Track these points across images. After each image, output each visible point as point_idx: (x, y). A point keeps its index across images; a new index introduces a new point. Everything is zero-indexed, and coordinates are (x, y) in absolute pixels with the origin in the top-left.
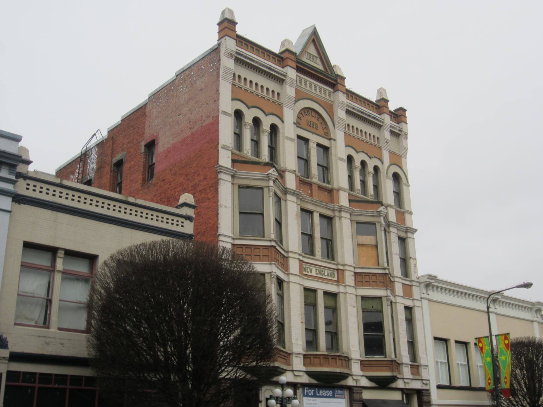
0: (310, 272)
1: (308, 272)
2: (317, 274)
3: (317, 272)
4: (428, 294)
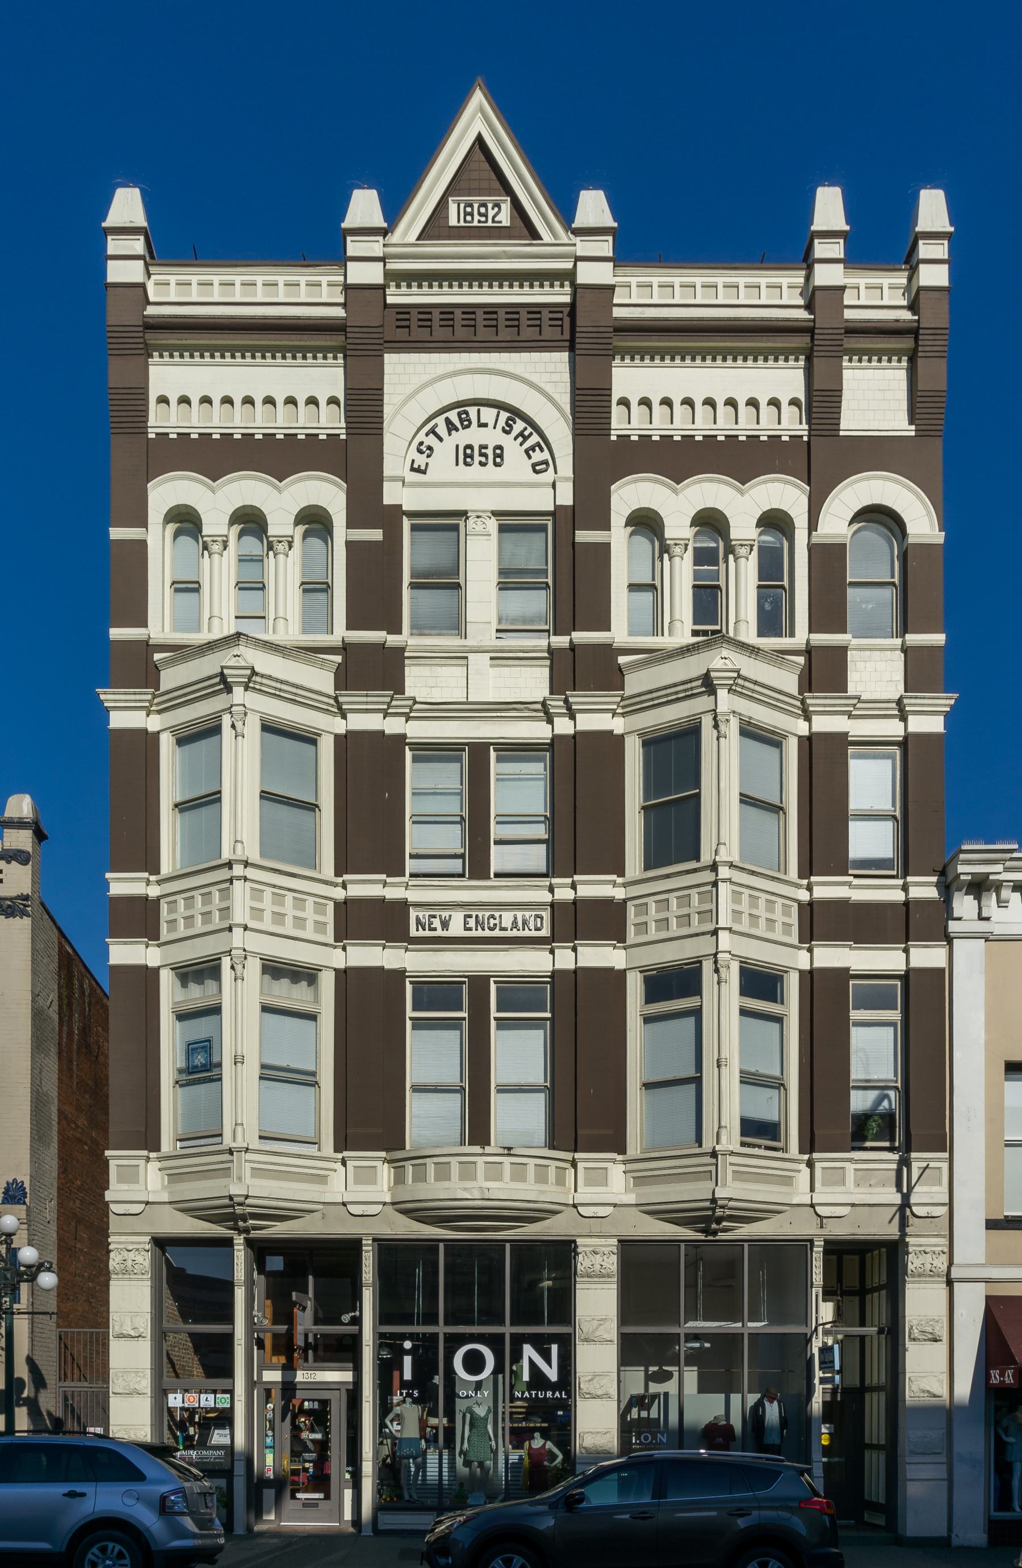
0: (439, 928)
1: (435, 929)
2: (467, 929)
3: (472, 923)
4: (988, 919)
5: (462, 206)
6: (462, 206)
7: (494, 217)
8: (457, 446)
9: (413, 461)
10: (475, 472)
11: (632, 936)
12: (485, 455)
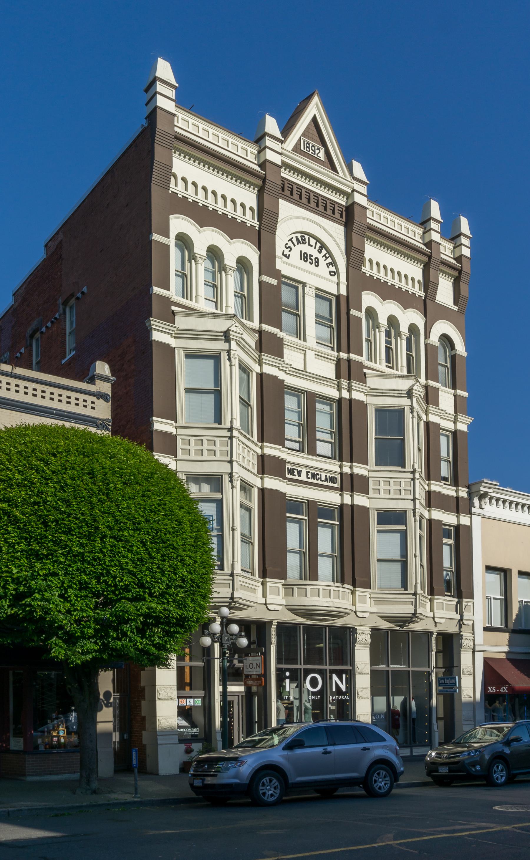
1: (295, 475)
2: (308, 478)
3: (310, 476)
5: (306, 142)
6: (306, 142)
7: (317, 154)
8: (301, 251)
9: (284, 251)
10: (307, 265)
11: (372, 494)
12: (312, 259)
